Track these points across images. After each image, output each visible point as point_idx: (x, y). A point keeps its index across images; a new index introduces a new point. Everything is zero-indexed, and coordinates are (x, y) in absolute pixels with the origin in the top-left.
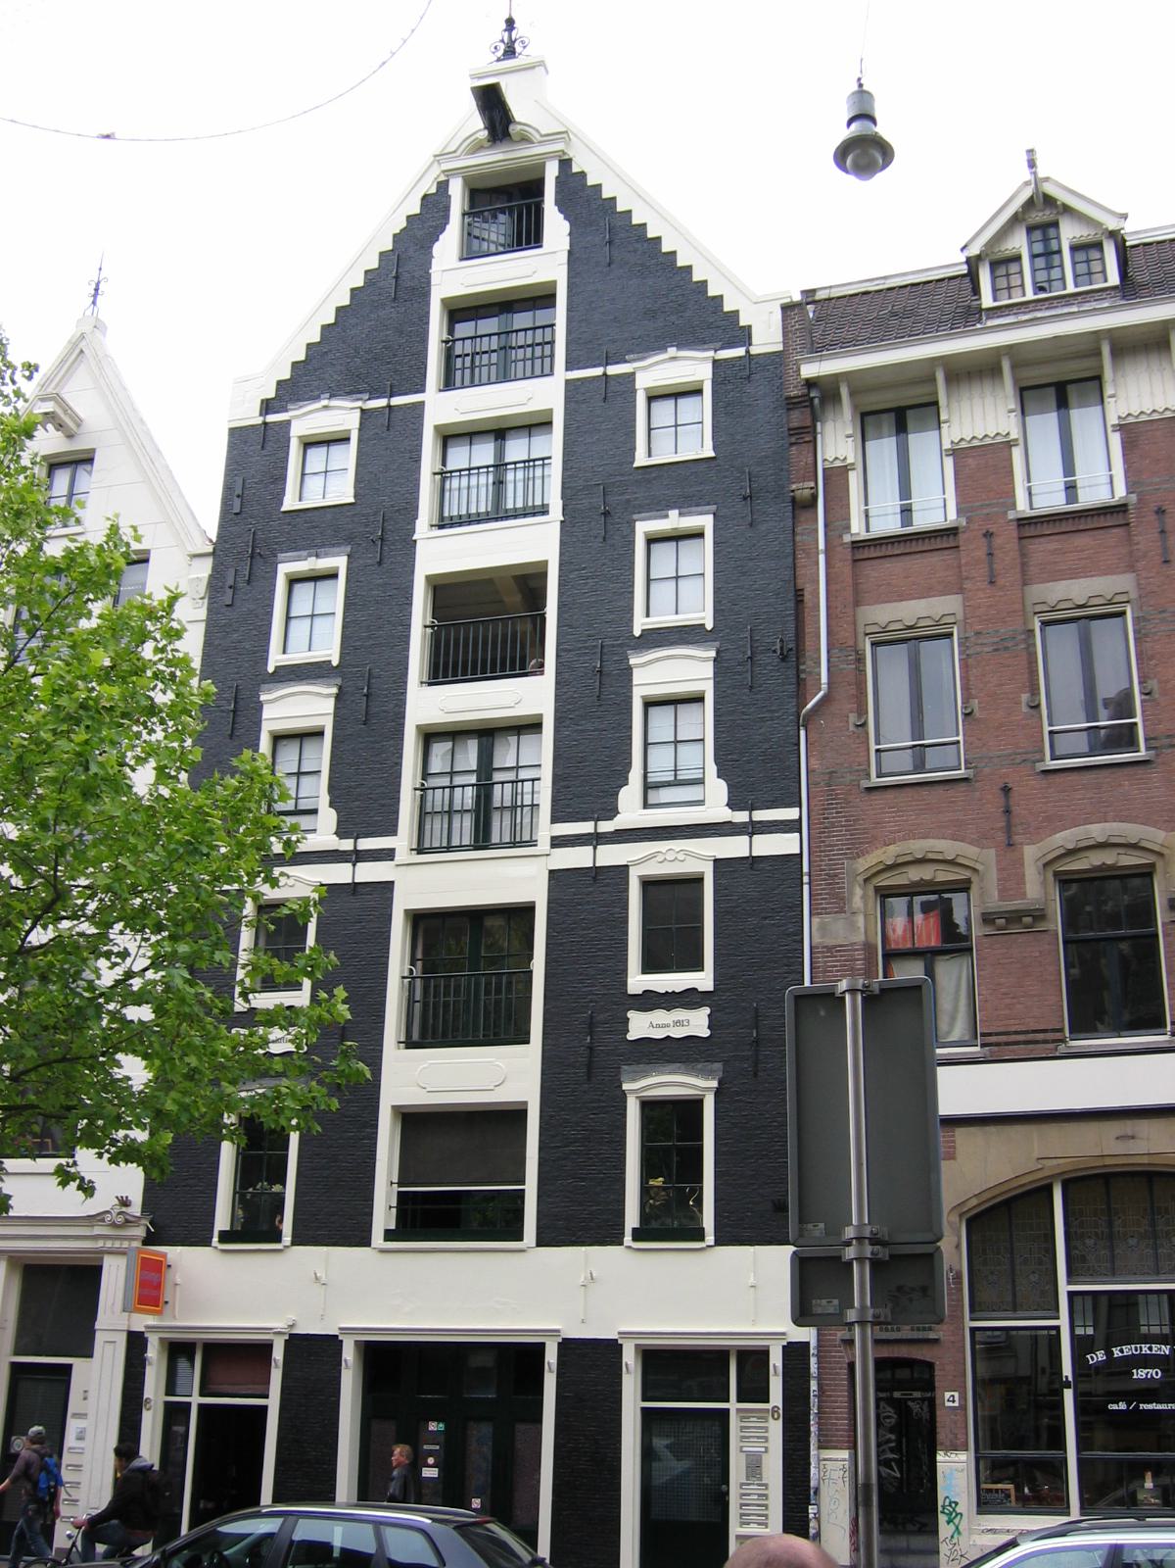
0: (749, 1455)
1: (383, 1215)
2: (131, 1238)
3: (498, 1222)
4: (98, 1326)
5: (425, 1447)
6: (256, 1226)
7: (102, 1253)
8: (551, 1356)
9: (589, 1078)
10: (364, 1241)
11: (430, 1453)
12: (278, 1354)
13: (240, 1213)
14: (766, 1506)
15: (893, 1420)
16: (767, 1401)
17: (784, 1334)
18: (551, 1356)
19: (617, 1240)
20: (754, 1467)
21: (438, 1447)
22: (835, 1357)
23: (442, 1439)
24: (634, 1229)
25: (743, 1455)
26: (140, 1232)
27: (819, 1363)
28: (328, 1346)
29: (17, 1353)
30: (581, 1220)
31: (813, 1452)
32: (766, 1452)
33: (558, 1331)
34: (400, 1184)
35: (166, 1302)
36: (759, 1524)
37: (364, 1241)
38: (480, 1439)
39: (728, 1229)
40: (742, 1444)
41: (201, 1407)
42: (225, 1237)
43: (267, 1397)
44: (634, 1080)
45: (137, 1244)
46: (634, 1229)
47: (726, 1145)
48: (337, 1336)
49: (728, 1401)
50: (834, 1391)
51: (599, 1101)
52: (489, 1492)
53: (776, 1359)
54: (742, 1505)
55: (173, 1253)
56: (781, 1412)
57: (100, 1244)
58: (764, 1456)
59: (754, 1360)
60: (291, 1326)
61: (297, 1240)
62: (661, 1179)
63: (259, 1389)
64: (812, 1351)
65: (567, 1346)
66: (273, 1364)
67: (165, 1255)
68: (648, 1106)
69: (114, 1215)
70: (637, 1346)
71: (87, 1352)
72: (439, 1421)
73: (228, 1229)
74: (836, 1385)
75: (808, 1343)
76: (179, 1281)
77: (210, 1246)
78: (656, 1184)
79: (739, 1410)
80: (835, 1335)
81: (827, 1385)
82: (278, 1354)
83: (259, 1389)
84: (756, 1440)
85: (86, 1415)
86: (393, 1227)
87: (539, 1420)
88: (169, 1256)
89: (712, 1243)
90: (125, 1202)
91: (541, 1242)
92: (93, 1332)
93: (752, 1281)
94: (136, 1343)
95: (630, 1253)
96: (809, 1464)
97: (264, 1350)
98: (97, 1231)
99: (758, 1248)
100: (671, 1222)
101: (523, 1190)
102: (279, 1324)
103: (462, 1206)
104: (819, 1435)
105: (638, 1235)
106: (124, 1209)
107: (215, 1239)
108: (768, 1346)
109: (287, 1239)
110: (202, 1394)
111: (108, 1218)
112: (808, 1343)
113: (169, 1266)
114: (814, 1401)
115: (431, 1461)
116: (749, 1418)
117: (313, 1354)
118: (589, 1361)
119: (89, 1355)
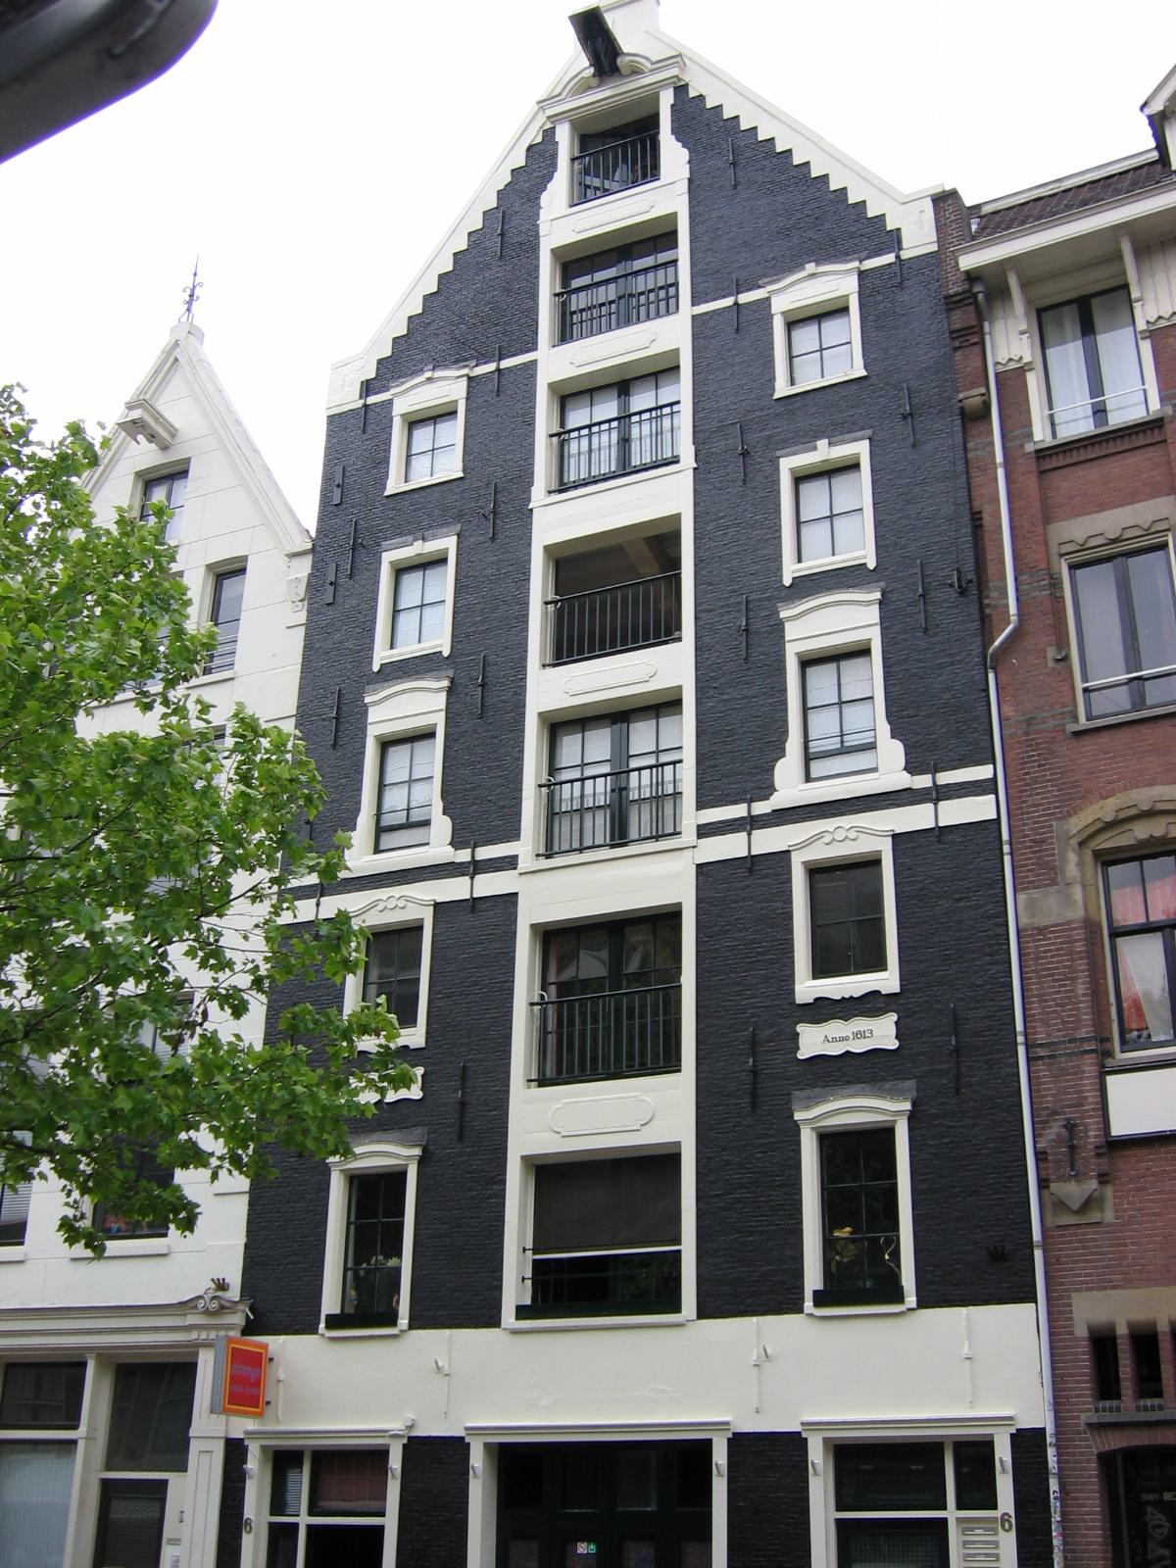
1: (515, 1288)
2: (229, 1327)
4: (192, 1433)
6: (368, 1309)
7: (197, 1346)
8: (720, 1456)
10: (493, 1321)
12: (395, 1462)
13: (353, 1293)
15: (1166, 1531)
16: (995, 1507)
17: (1011, 1418)
18: (720, 1456)
22: (1080, 1446)
24: (816, 1293)
26: (238, 1319)
27: (1059, 1455)
28: (454, 1449)
30: (749, 1283)
33: (727, 1423)
34: (535, 1251)
35: (268, 1403)
37: (493, 1321)
39: (934, 1287)
41: (310, 1527)
42: (334, 1322)
43: (382, 1514)
44: (807, 1108)
45: (235, 1334)
46: (816, 1293)
48: (463, 1438)
49: (944, 1508)
53: (1003, 1452)
55: (275, 1343)
56: (1013, 1521)
57: (194, 1335)
59: (975, 1456)
60: (410, 1427)
61: (416, 1323)
62: (848, 1229)
64: (1049, 1440)
65: (739, 1443)
66: (389, 1474)
67: (265, 1346)
70: (826, 1440)
71: (181, 1466)
73: (338, 1312)
74: (1083, 1484)
75: (1044, 1429)
76: (282, 1376)
78: (842, 1235)
79: (958, 1520)
80: (1078, 1417)
81: (1071, 1484)
82: (395, 1462)
85: (179, 1540)
86: (528, 1302)
87: (706, 1537)
88: (270, 1348)
89: (914, 1305)
90: (222, 1286)
91: (703, 1313)
92: (186, 1441)
93: (966, 1351)
94: (235, 1451)
97: (381, 1455)
98: (191, 1320)
100: (859, 1282)
101: (679, 1251)
102: (396, 1425)
104: (1065, 1551)
105: (820, 1299)
106: (220, 1293)
107: (322, 1325)
108: (992, 1435)
109: (403, 1321)
110: (311, 1513)
112: (1044, 1429)
113: (271, 1359)
114: (1055, 1505)
116: (973, 1529)
117: (436, 1460)
118: (770, 1459)
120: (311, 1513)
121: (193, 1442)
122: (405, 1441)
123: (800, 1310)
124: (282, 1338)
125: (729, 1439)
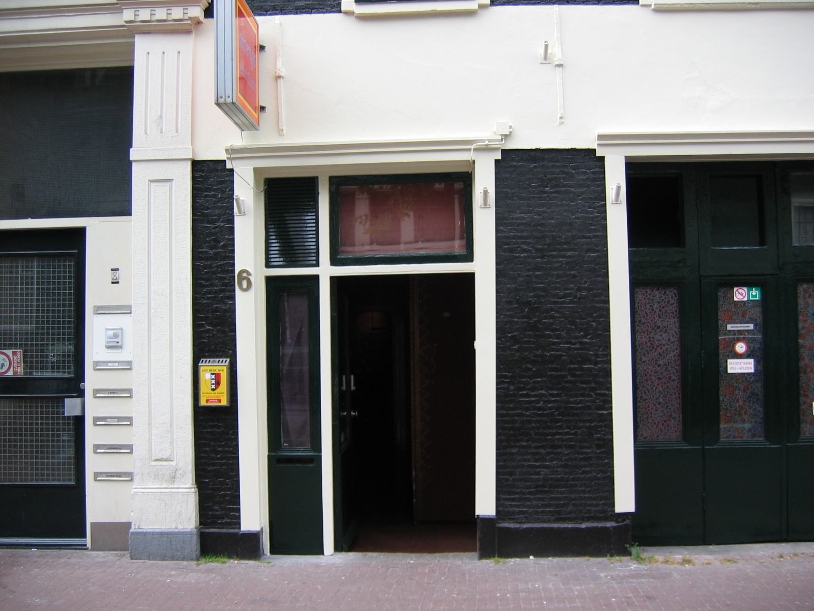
4: (134, 154)
11: (739, 336)
21: (751, 327)
23: (757, 313)
41: (336, 282)
60: (506, 137)
71: (118, 203)
83: (457, 246)
92: (129, 164)
94: (210, 182)
97: (459, 182)
110: (335, 261)
115: (741, 347)
117: (547, 181)
119: (124, 209)
120: (335, 261)
121: (136, 169)
122: (499, 156)
124: (278, 19)
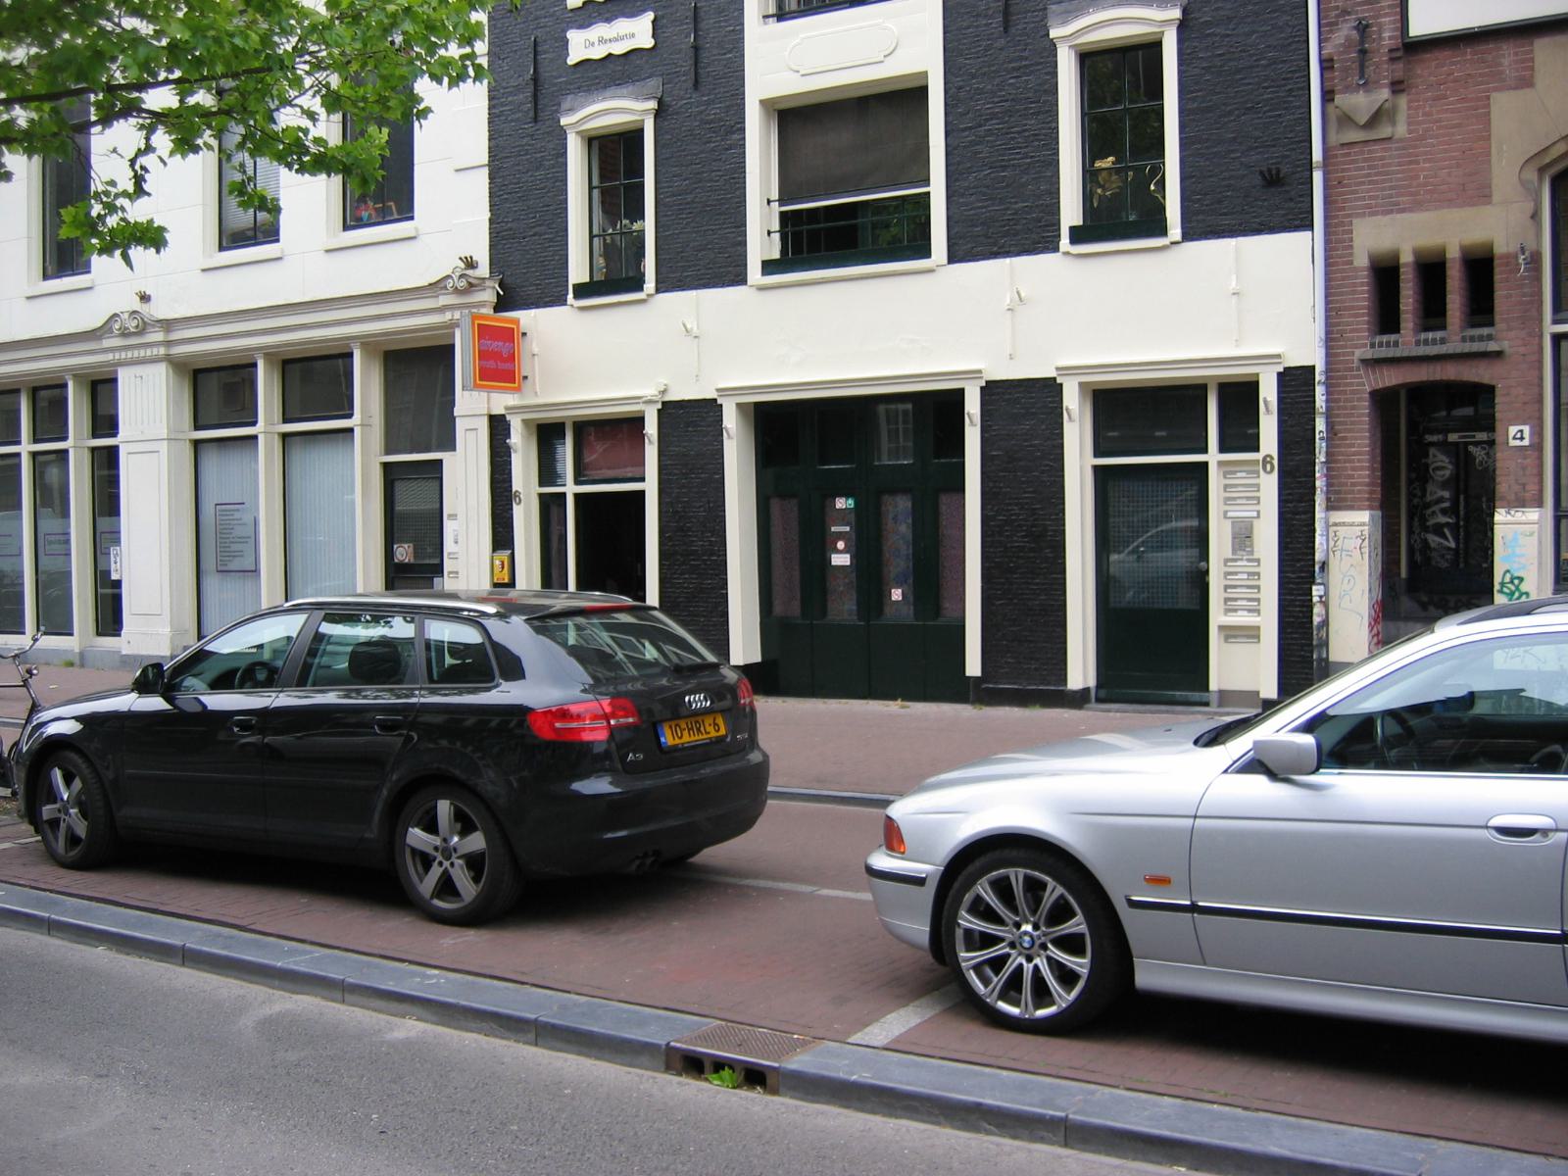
0: (1235, 522)
1: (761, 238)
2: (482, 304)
3: (896, 235)
5: (833, 529)
6: (616, 277)
7: (453, 325)
8: (973, 406)
9: (1006, 30)
10: (740, 279)
11: (840, 536)
12: (651, 428)
13: (600, 262)
14: (1258, 587)
15: (1447, 473)
16: (1257, 449)
17: (1278, 356)
18: (973, 406)
19: (1050, 245)
20: (1243, 537)
21: (848, 529)
22: (1352, 384)
23: (852, 518)
24: (1073, 229)
25: (1228, 523)
26: (488, 296)
27: (1328, 393)
28: (708, 410)
29: (388, 452)
30: (1005, 220)
31: (1319, 514)
32: (1258, 517)
33: (980, 372)
34: (782, 201)
35: (525, 378)
36: (1249, 611)
37: (740, 279)
38: (899, 510)
39: (1200, 217)
40: (1227, 508)
41: (578, 497)
42: (582, 291)
43: (642, 479)
44: (1065, 23)
45: (488, 311)
46: (1073, 229)
47: (1194, 99)
48: (715, 400)
49: (1205, 450)
50: (1350, 431)
51: (1022, 58)
52: (911, 581)
53: (1269, 392)
54: (1226, 587)
55: (527, 318)
56: (1276, 462)
57: (448, 316)
58: (1256, 522)
59: (1240, 397)
60: (663, 392)
61: (662, 286)
62: (1111, 159)
63: (629, 472)
64: (1317, 378)
65: (993, 390)
66: (646, 441)
67: (517, 322)
68: (1088, 59)
69: (456, 279)
70: (1081, 385)
71: (449, 444)
72: (847, 496)
73: (587, 280)
74: (1352, 423)
75: (1314, 367)
76: (536, 350)
77: (566, 305)
78: (1104, 166)
79: (1221, 464)
80: (1353, 353)
81: (1341, 423)
82: (651, 428)
83: (629, 472)
84: (1243, 499)
85: (456, 515)
86: (776, 255)
87: (960, 488)
88: (522, 322)
89: (1178, 237)
90: (471, 264)
91: (953, 257)
93: (1233, 285)
94: (498, 426)
95: (1068, 261)
96: (1314, 531)
97: (637, 422)
98: (444, 300)
99: (1241, 239)
100: (1122, 215)
101: (929, 193)
102: (650, 391)
103: (859, 220)
104: (1328, 492)
105: (1078, 235)
106: (470, 272)
107: (570, 295)
108: (1258, 374)
109: (650, 285)
110: (577, 482)
111: (450, 284)
112: (1314, 367)
113: (524, 334)
114: (1321, 447)
115: (841, 545)
116: (1235, 472)
117: (690, 423)
118: (1023, 406)
119: (453, 448)
120: (577, 482)
121: (458, 421)
122: (660, 406)
123: (1056, 249)
124: (533, 312)
125: (982, 388)
